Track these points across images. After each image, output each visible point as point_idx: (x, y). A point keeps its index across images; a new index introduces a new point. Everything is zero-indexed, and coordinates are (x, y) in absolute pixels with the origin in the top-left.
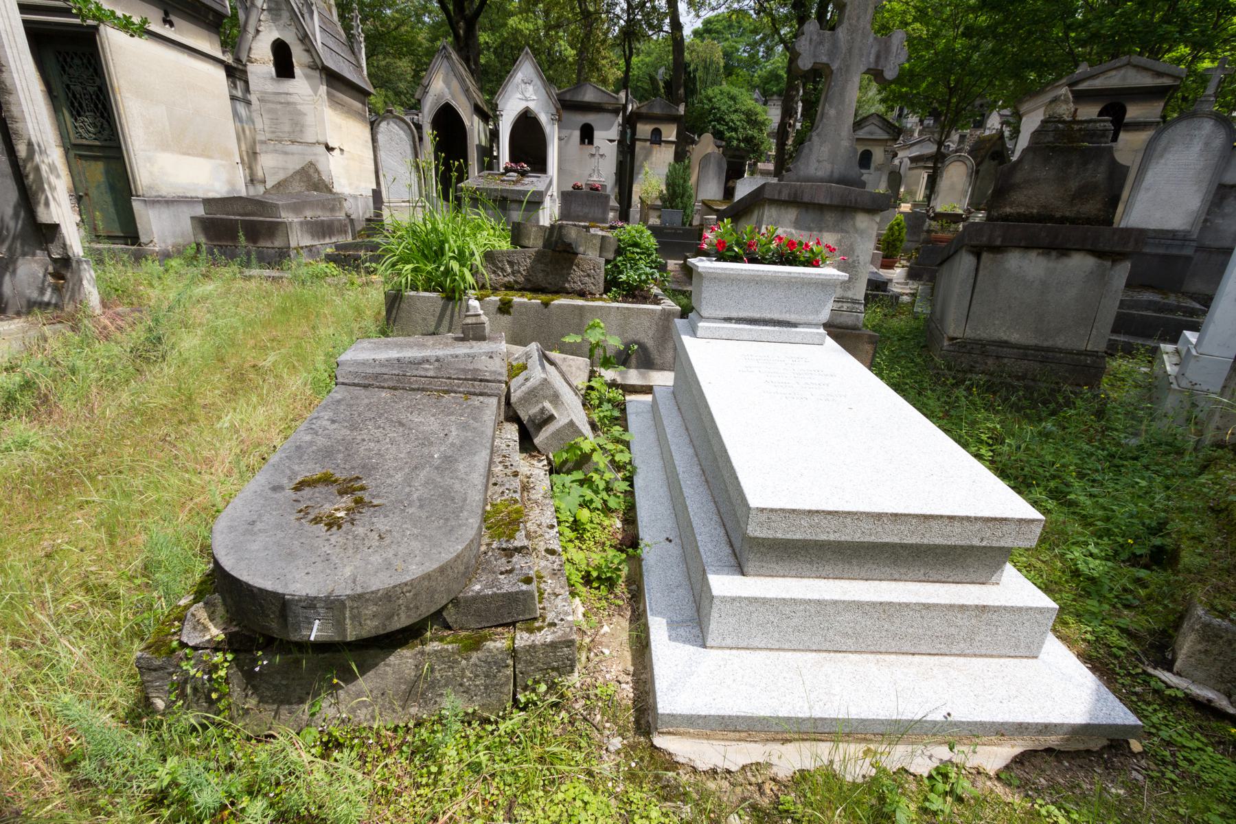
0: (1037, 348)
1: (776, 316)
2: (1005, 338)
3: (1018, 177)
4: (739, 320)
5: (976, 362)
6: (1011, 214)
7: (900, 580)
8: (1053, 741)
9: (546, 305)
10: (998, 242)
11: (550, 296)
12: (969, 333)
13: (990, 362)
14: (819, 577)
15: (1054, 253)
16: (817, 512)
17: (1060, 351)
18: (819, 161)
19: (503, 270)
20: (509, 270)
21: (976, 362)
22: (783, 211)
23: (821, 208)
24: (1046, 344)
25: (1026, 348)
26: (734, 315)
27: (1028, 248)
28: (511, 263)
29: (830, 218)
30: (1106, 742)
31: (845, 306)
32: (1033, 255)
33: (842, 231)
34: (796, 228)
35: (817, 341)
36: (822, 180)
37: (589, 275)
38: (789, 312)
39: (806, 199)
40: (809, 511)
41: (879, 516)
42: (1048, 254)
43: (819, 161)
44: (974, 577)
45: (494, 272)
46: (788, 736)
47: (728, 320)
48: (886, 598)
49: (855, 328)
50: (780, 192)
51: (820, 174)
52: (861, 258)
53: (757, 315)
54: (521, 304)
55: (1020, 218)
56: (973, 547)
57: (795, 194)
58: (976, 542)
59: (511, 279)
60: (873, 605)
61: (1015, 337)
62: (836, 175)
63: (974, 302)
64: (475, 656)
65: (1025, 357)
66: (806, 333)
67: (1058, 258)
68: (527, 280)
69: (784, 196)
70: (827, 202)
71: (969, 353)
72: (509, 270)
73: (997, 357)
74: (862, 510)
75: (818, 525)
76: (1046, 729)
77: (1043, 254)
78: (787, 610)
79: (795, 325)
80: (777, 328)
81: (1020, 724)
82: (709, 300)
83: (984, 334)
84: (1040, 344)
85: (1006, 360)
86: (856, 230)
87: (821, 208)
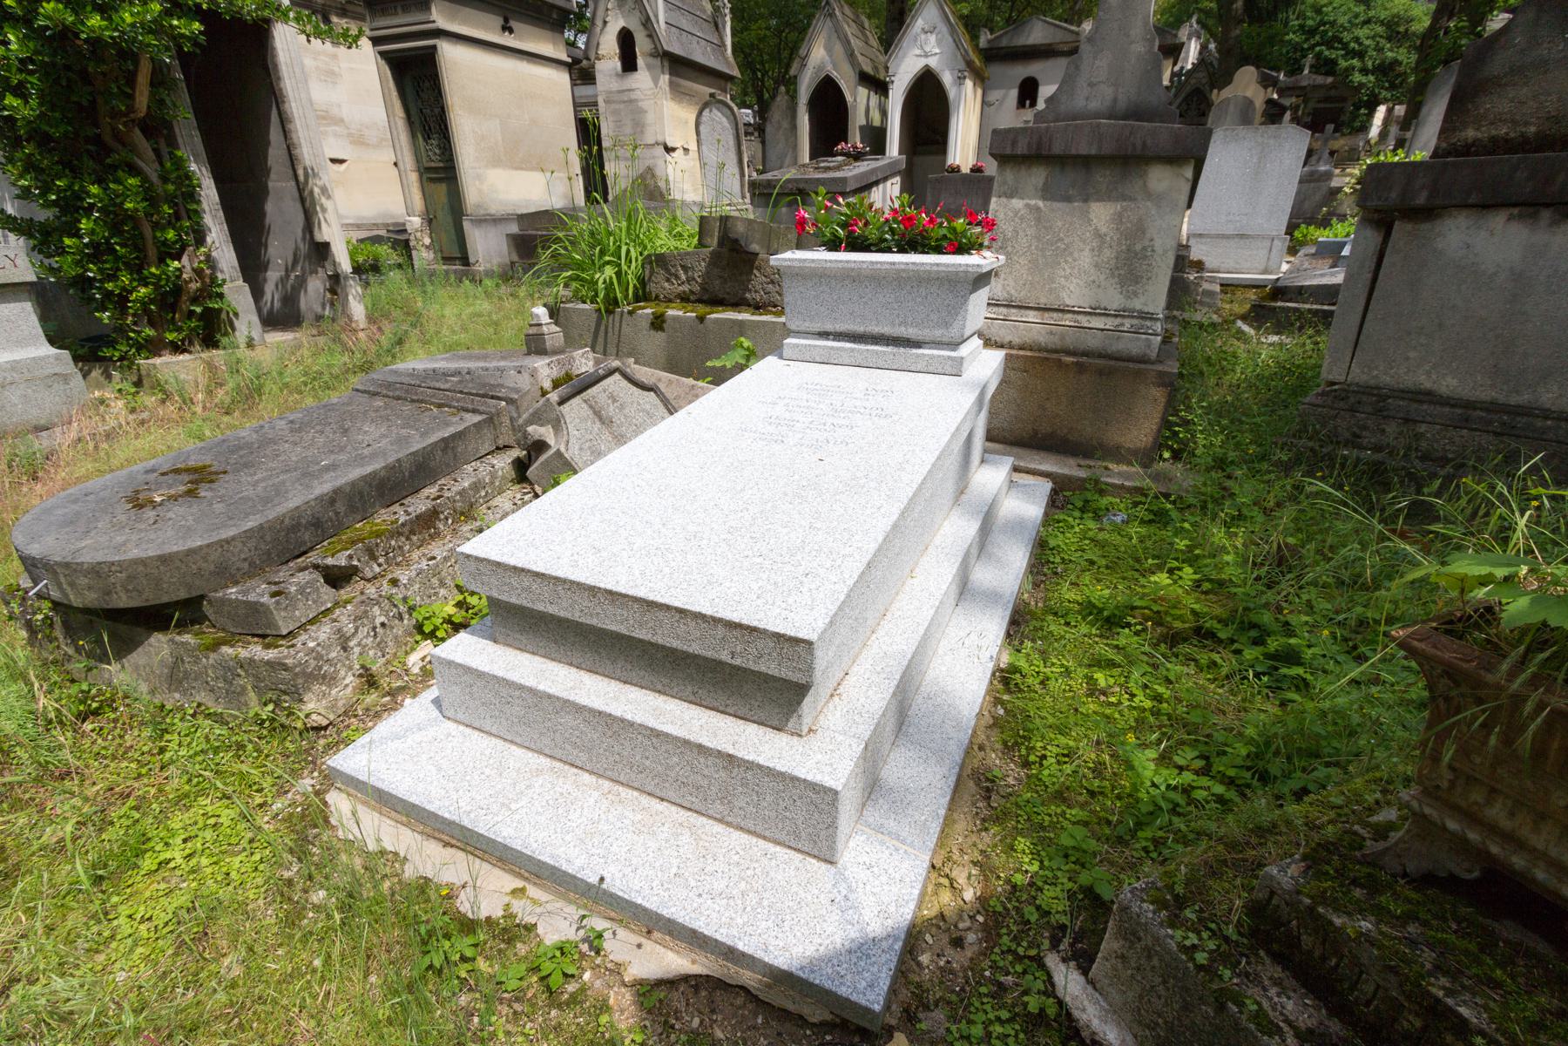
0: (1493, 407)
1: (887, 330)
2: (1428, 385)
3: (1497, 65)
4: (839, 336)
5: (1365, 428)
6: (1475, 142)
7: (665, 694)
8: (748, 978)
9: (701, 319)
10: (1421, 199)
11: (708, 309)
12: (1359, 375)
13: (1392, 428)
14: (571, 664)
15: (1546, 214)
16: (523, 570)
17: (1546, 414)
18: (1091, 85)
19: (677, 277)
20: (683, 277)
21: (1365, 428)
22: (1023, 172)
23: (1087, 162)
24: (1514, 400)
25: (1469, 405)
26: (829, 327)
27: (1486, 206)
28: (685, 268)
29: (1102, 177)
30: (828, 1017)
31: (1127, 323)
32: (1498, 220)
33: (1124, 198)
34: (1044, 198)
35: (949, 370)
36: (1097, 115)
37: (772, 282)
38: (904, 323)
39: (1057, 149)
40: (515, 568)
41: (593, 590)
42: (1534, 216)
43: (1091, 85)
44: (763, 716)
45: (668, 280)
46: (454, 842)
47: (824, 335)
48: (616, 710)
49: (1142, 360)
50: (1014, 143)
51: (1094, 105)
52: (1158, 244)
53: (860, 329)
54: (676, 318)
55: (1497, 146)
56: (721, 663)
57: (1039, 144)
58: (725, 656)
59: (686, 288)
60: (592, 711)
61: (1448, 384)
62: (1122, 105)
63: (1370, 316)
64: (212, 655)
65: (1464, 423)
66: (932, 357)
67: (1554, 223)
68: (704, 289)
69: (1021, 149)
70: (1093, 152)
71: (1352, 410)
72: (683, 277)
73: (1407, 421)
74: (572, 578)
75: (528, 590)
76: (730, 954)
77: (1521, 217)
78: (504, 692)
79: (918, 344)
80: (889, 349)
81: (694, 932)
82: (798, 306)
83: (1387, 376)
84: (1502, 399)
85: (1423, 428)
86: (1149, 195)
87: (1087, 162)
